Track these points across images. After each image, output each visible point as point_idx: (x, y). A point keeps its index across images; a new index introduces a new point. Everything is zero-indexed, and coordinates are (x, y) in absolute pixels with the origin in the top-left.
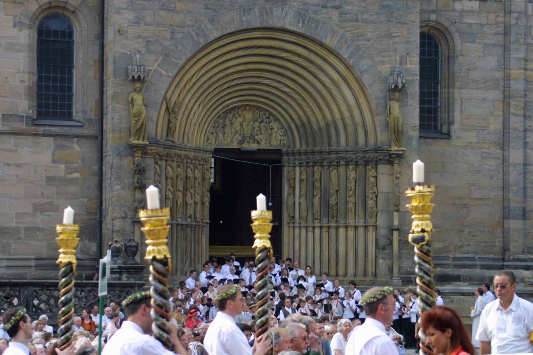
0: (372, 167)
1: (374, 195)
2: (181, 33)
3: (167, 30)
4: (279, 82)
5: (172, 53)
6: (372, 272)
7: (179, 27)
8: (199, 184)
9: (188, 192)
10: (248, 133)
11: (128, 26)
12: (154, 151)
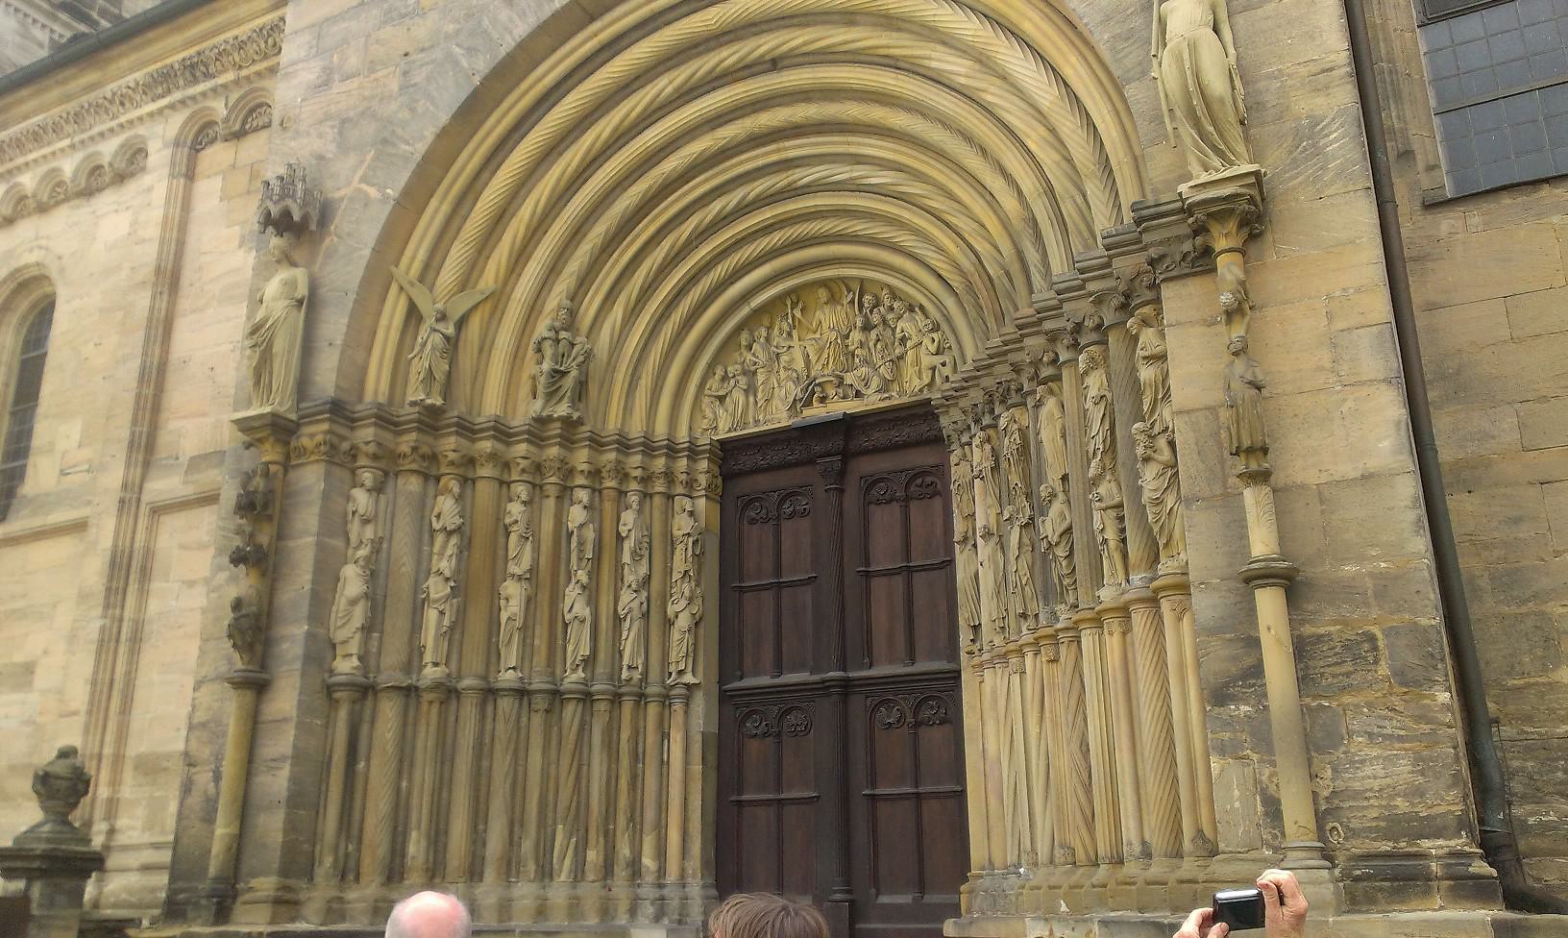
0: (1145, 323)
1: (1162, 442)
2: (428, 63)
3: (395, 72)
4: (858, 160)
5: (400, 131)
6: (1200, 831)
7: (423, 50)
8: (636, 555)
9: (573, 581)
10: (826, 373)
11: (302, 100)
12: (320, 438)
